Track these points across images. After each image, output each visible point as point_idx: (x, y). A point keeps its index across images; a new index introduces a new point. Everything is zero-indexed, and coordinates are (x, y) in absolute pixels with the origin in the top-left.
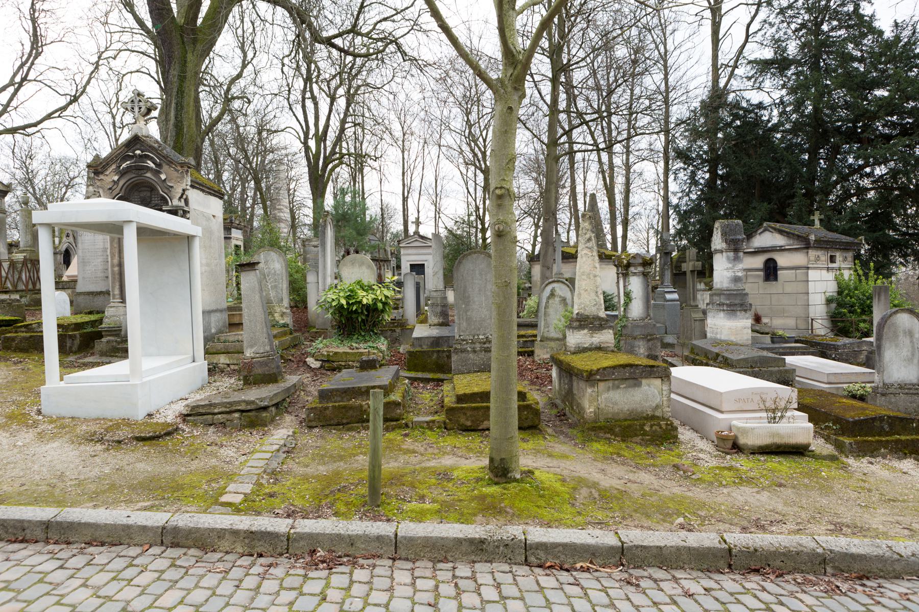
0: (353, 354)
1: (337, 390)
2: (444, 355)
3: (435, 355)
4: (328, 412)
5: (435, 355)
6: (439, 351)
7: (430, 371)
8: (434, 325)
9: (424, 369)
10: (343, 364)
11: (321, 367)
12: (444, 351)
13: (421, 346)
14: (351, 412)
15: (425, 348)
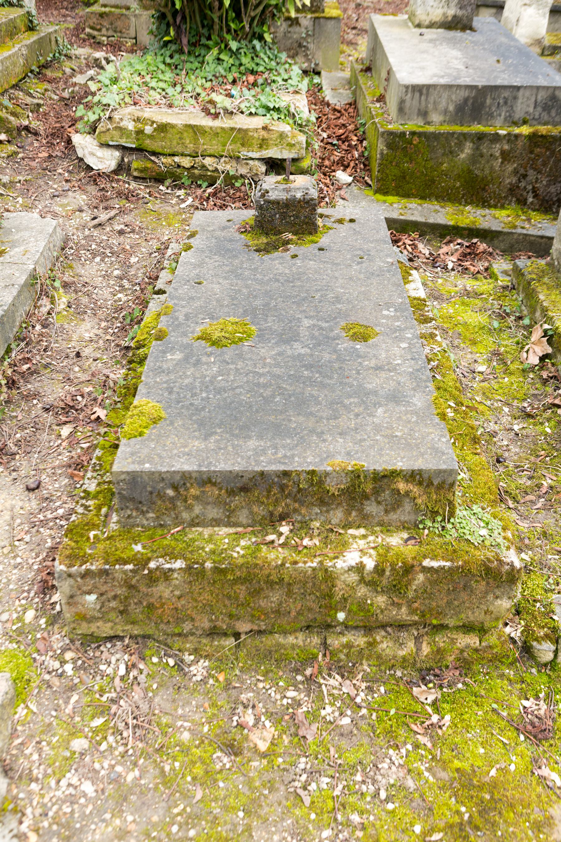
0: (215, 133)
1: (206, 480)
2: (496, 149)
3: (468, 149)
4: (162, 590)
5: (468, 149)
6: (480, 137)
7: (446, 196)
8: (431, 25)
9: (427, 190)
10: (186, 162)
11: (121, 168)
12: (496, 138)
13: (424, 114)
14: (275, 597)
15: (438, 124)
